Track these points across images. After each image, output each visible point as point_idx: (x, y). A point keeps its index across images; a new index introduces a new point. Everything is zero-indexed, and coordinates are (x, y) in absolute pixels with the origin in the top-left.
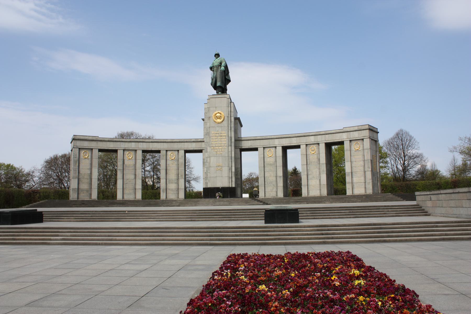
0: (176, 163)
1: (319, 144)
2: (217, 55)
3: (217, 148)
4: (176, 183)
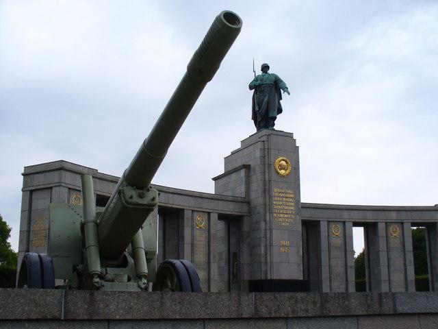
0: (205, 234)
1: (402, 223)
2: (265, 68)
3: (282, 216)
4: (205, 270)
